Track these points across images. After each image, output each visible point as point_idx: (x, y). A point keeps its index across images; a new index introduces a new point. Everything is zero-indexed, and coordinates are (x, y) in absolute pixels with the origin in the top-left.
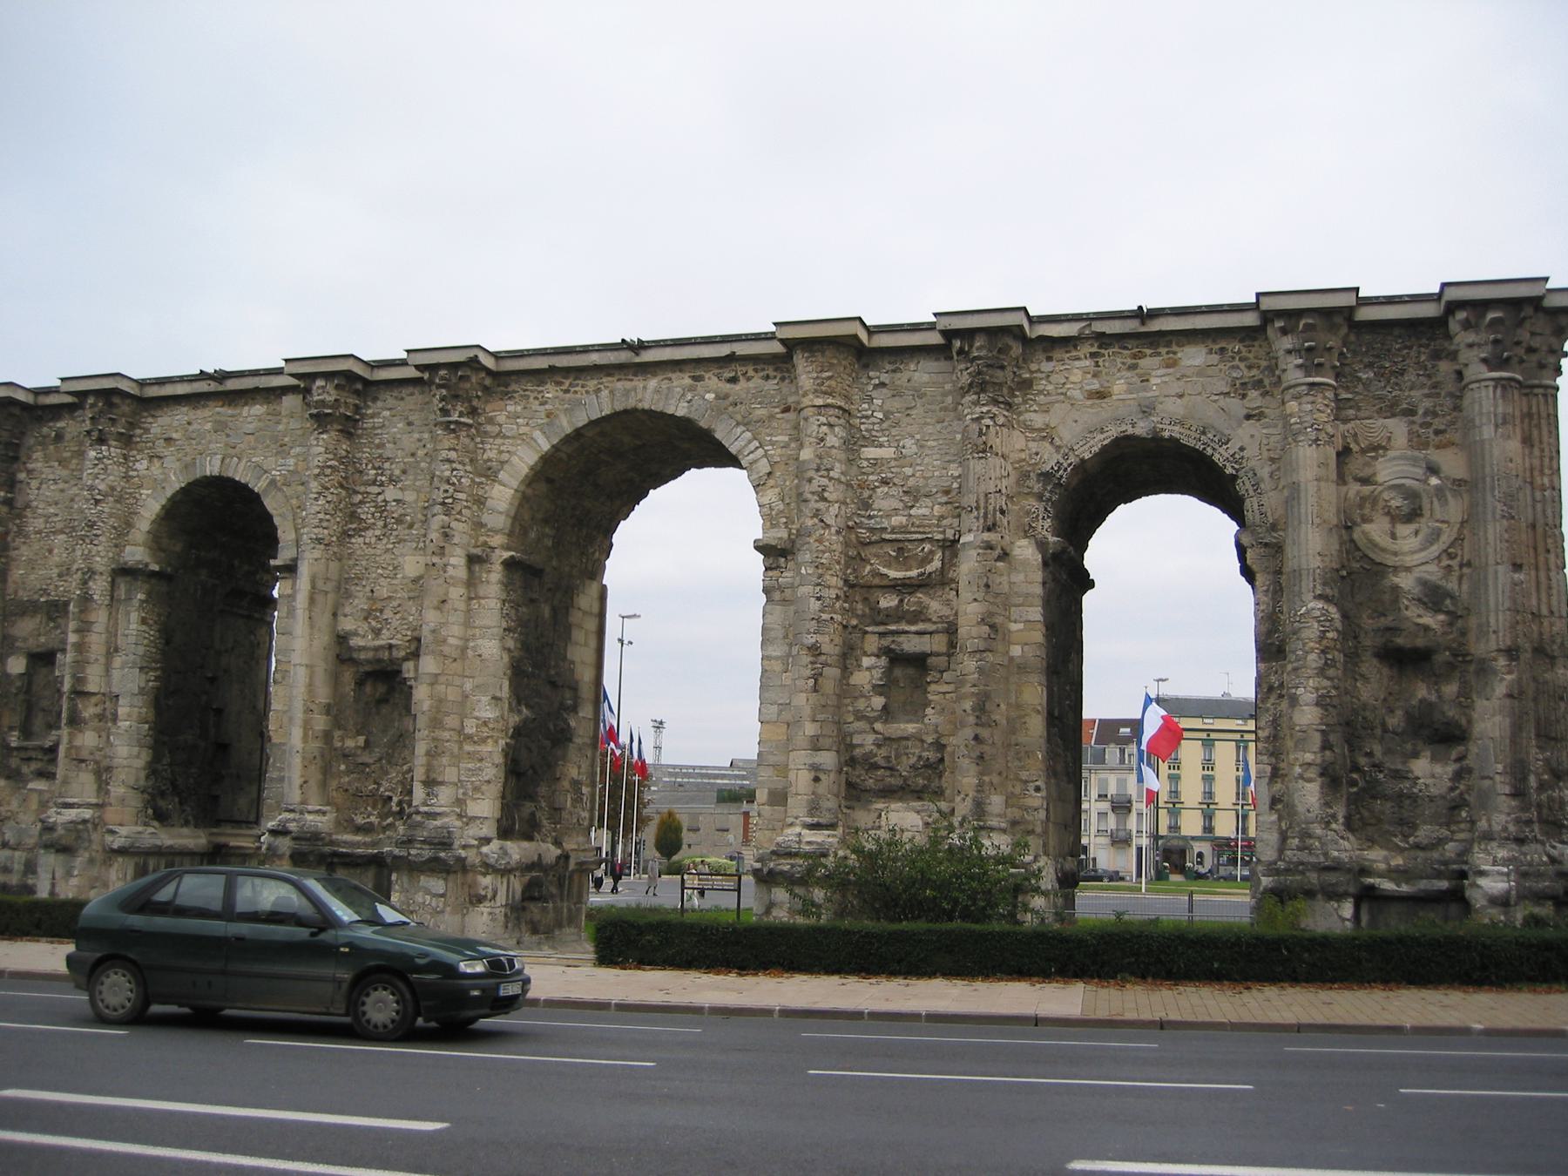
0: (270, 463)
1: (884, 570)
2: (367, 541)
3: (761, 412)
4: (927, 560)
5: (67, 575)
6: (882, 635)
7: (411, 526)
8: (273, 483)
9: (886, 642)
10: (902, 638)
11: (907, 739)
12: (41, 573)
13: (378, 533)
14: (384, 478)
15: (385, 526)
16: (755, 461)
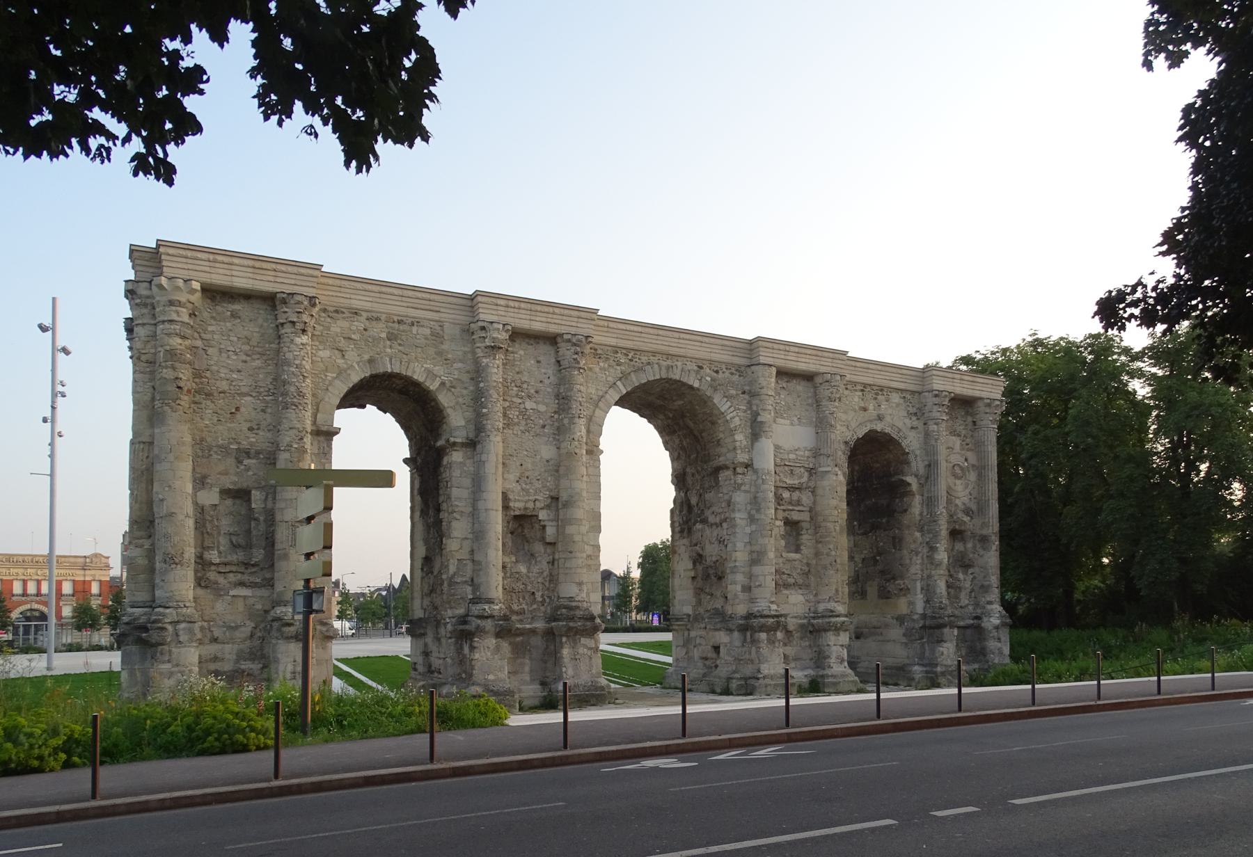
0: (438, 370)
1: (785, 480)
2: (515, 432)
3: (733, 392)
4: (801, 477)
5: (258, 429)
6: (784, 510)
7: (544, 427)
8: (443, 384)
9: (786, 514)
10: (793, 513)
11: (795, 560)
12: (229, 425)
13: (522, 428)
14: (523, 394)
15: (527, 424)
16: (734, 417)
